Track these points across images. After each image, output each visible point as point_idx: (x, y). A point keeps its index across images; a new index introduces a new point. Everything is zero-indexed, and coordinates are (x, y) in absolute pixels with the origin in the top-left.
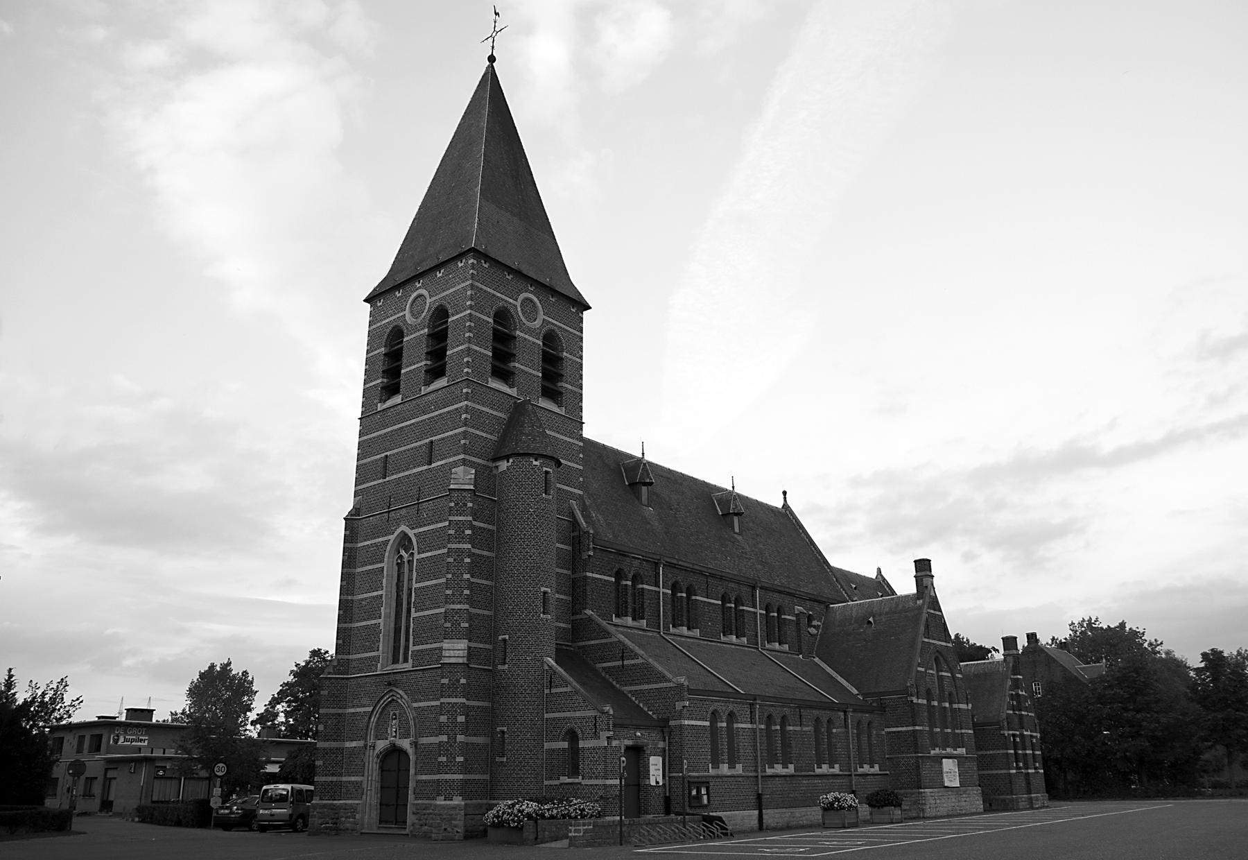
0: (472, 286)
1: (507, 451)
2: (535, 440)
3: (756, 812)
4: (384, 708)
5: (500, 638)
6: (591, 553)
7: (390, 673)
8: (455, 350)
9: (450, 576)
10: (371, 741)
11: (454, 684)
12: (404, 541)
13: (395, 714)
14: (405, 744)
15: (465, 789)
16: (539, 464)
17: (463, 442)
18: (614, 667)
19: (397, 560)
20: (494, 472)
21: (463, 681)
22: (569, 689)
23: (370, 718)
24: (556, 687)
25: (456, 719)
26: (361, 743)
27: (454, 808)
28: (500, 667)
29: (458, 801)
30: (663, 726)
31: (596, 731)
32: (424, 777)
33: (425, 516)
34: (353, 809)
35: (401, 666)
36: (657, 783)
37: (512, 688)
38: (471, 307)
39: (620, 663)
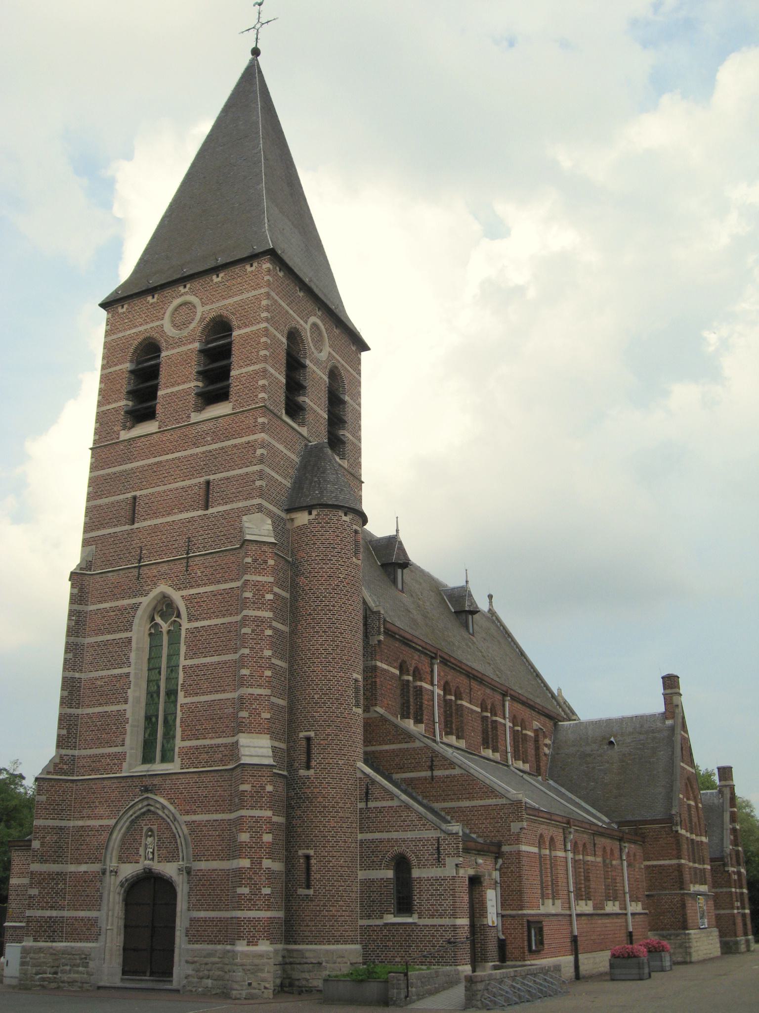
0: (268, 295)
1: (309, 501)
2: (342, 490)
3: (571, 958)
4: (133, 822)
5: (302, 735)
6: (382, 638)
7: (145, 775)
8: (244, 370)
9: (246, 651)
10: (112, 863)
11: (258, 792)
12: (165, 607)
13: (151, 830)
14: (169, 870)
15: (269, 931)
16: (348, 520)
17: (258, 483)
18: (419, 779)
19: (150, 629)
20: (288, 526)
21: (269, 788)
22: (395, 803)
23: (111, 834)
24: (376, 799)
25: (261, 838)
26: (96, 867)
27: (261, 956)
28: (302, 772)
29: (264, 947)
30: (494, 850)
31: (439, 857)
32: (202, 914)
33: (200, 574)
34: (85, 959)
35: (159, 767)
36: (493, 922)
37: (320, 799)
38: (267, 320)
39: (428, 774)
